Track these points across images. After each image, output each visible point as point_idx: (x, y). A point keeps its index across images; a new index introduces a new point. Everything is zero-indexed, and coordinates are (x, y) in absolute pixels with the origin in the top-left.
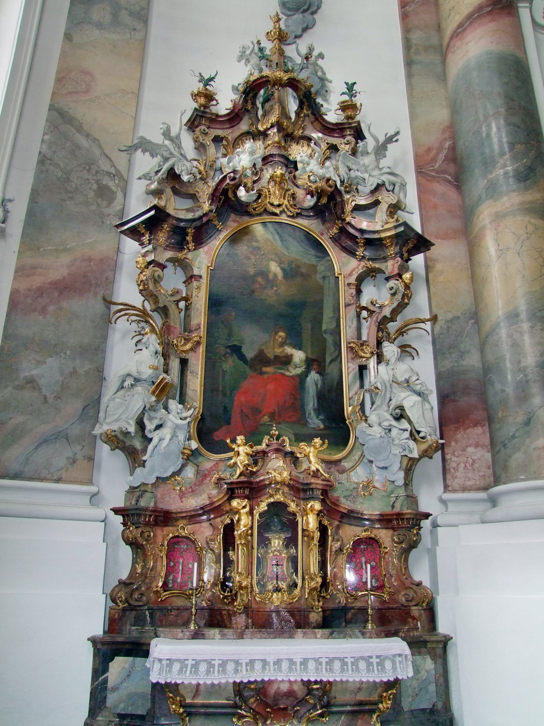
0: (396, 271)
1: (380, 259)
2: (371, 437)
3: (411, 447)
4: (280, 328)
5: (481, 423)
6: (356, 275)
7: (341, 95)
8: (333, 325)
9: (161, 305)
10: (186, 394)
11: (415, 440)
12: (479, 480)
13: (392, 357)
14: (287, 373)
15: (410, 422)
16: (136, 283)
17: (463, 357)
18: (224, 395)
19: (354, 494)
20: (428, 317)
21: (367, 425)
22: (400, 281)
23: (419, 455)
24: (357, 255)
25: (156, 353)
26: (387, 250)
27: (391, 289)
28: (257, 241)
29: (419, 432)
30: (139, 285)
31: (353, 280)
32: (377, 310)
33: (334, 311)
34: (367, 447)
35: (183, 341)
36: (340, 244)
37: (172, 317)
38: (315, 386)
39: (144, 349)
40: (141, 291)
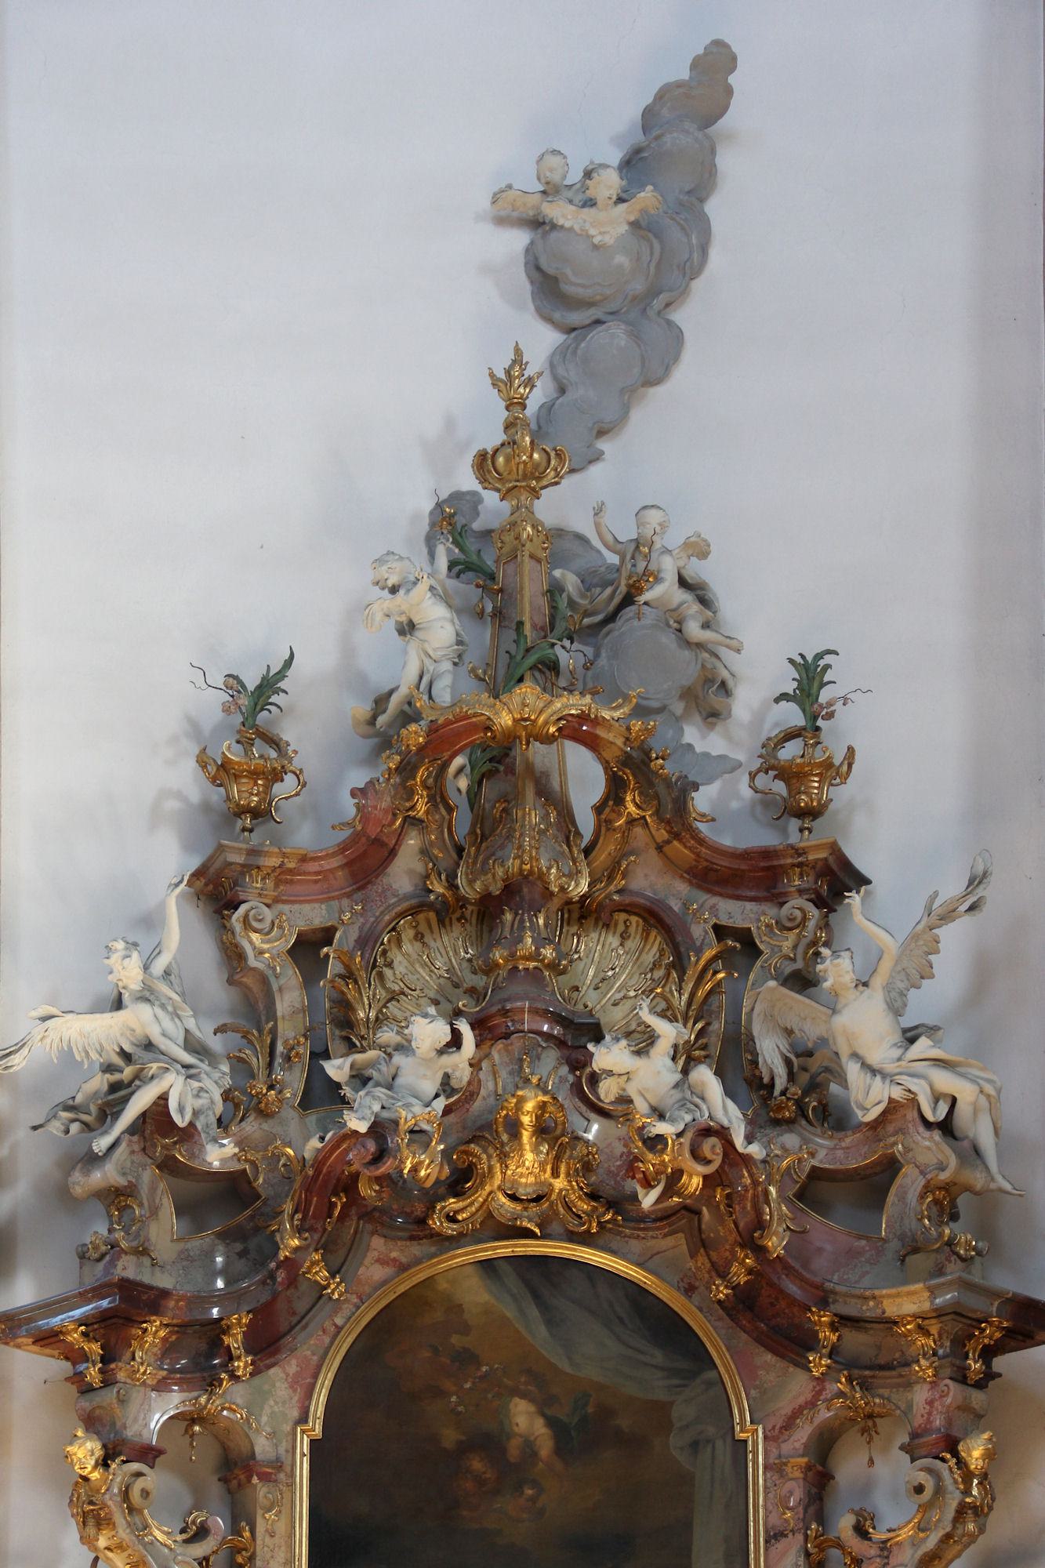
7: (777, 700)
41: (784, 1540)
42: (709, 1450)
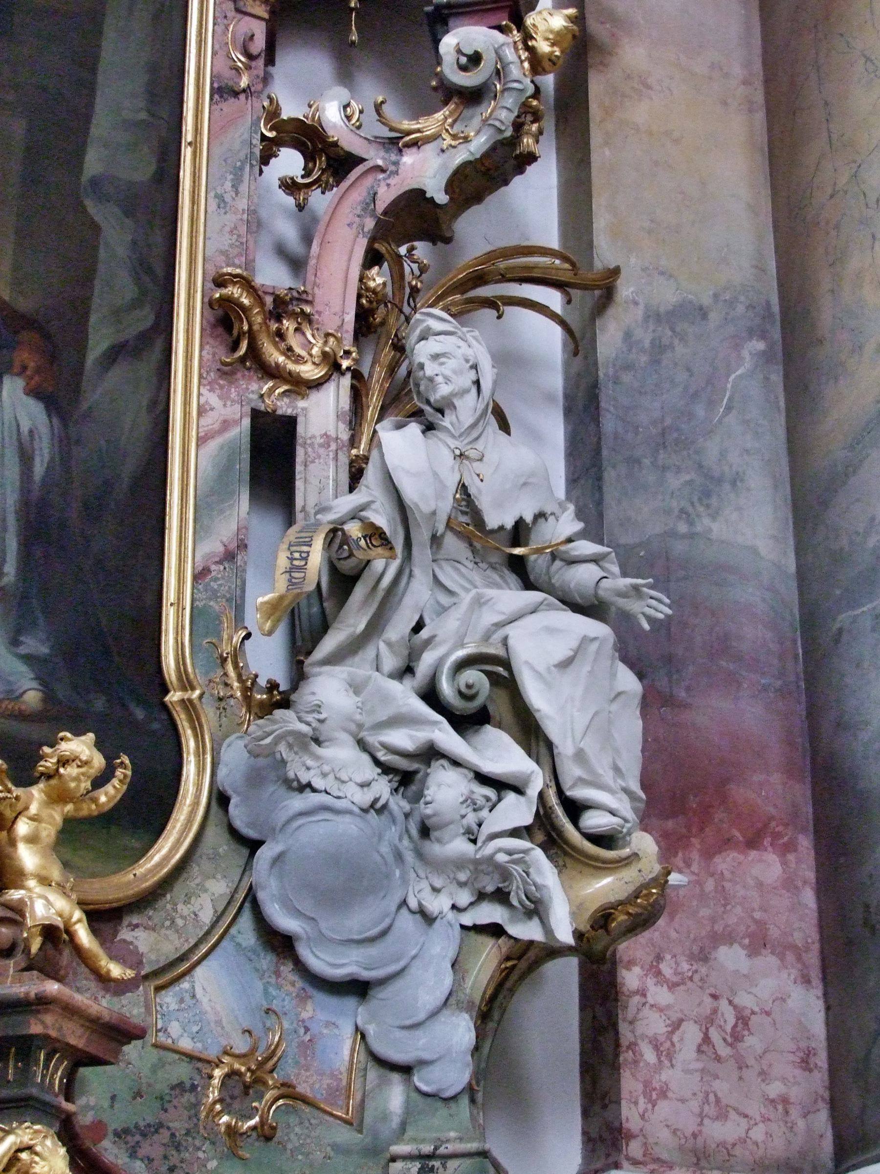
5: (776, 836)
12: (766, 1120)
17: (714, 501)
19: (178, 1123)
22: (516, 35)
34: (278, 859)
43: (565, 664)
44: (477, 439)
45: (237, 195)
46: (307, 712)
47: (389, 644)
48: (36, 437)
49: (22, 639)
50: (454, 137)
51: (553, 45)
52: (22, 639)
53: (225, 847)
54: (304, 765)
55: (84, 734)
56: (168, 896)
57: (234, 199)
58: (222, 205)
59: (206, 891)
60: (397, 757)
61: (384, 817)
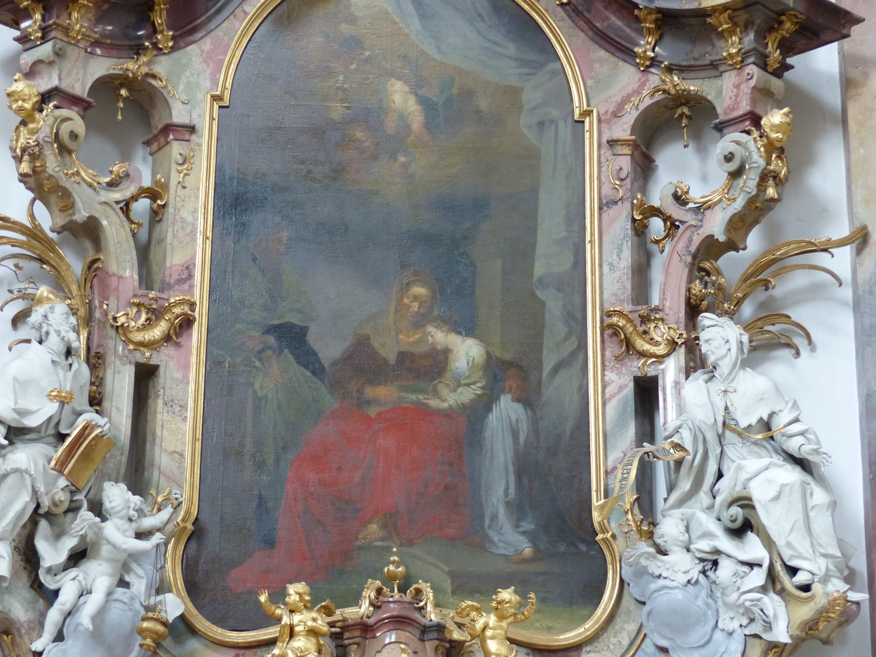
0: (744, 107)
1: (702, 68)
2: (661, 582)
3: (770, 612)
4: (416, 273)
6: (635, 114)
8: (566, 262)
9: (81, 215)
10: (152, 465)
11: (782, 592)
13: (722, 357)
14: (434, 403)
15: (769, 543)
16: (9, 154)
18: (260, 466)
20: (842, 230)
21: (652, 550)
22: (756, 134)
23: (791, 637)
24: (635, 55)
25: (69, 352)
26: (721, 43)
27: (729, 158)
28: (352, 20)
29: (793, 571)
30: (19, 160)
31: (623, 130)
32: (690, 219)
33: (568, 221)
35: (144, 316)
36: (588, 22)
37: (112, 249)
38: (509, 440)
39: (35, 344)
40: (23, 178)
41: (614, 208)
42: (553, 128)
43: (777, 498)
44: (732, 381)
45: (620, 260)
46: (659, 538)
47: (704, 492)
48: (520, 422)
49: (521, 524)
50: (729, 199)
51: (777, 133)
52: (521, 524)
53: (633, 607)
54: (656, 565)
55: (509, 587)
56: (605, 635)
57: (618, 263)
58: (612, 268)
59: (625, 630)
60: (705, 554)
61: (697, 587)
